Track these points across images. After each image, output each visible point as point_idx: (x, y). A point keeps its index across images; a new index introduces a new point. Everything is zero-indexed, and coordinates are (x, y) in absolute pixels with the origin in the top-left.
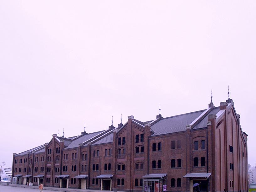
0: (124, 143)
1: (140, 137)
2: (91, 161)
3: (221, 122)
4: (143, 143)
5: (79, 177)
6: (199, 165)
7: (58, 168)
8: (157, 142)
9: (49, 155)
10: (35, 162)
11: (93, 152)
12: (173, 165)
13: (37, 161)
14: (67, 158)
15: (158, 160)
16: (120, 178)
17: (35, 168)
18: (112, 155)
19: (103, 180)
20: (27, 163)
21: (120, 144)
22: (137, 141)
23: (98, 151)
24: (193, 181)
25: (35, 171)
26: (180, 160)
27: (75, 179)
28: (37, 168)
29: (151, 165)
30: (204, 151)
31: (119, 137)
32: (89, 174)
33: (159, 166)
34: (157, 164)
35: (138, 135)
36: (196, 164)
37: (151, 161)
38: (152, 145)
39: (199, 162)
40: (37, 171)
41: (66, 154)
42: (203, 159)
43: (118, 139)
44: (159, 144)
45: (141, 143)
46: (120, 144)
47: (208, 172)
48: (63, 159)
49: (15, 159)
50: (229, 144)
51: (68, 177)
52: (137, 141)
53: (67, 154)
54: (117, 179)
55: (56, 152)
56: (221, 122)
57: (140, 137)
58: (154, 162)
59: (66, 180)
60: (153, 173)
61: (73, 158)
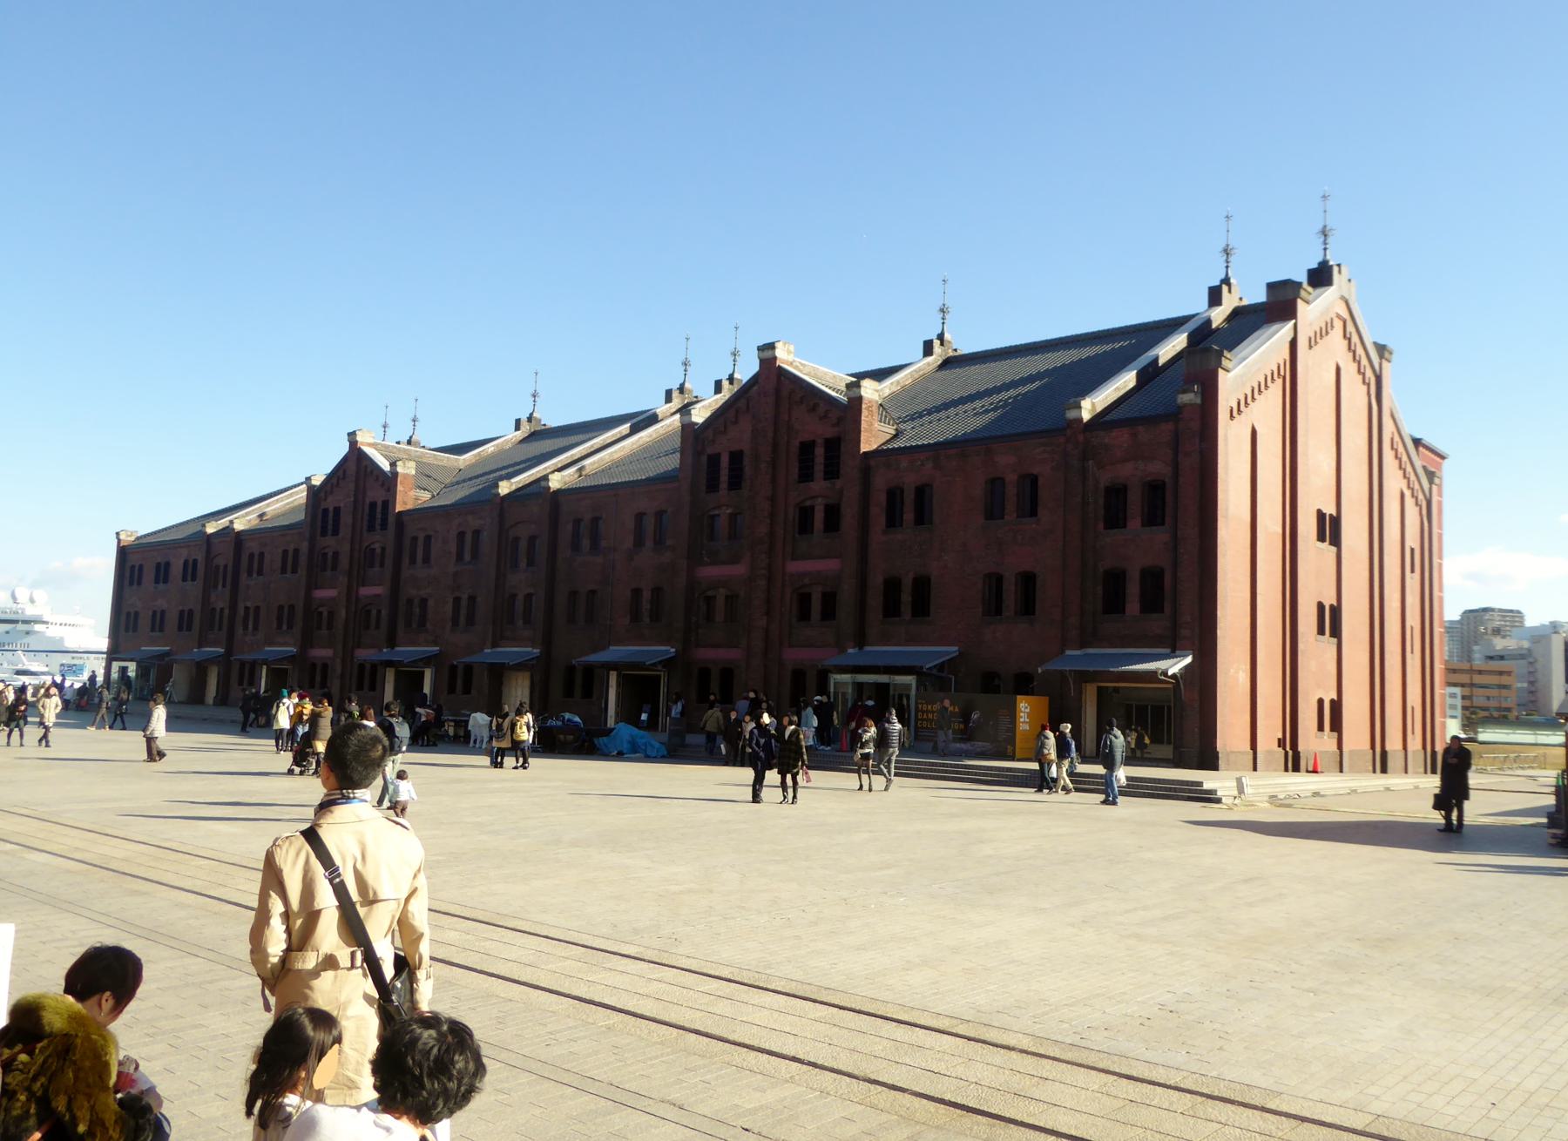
0: (736, 482)
1: (819, 451)
3: (1260, 389)
4: (839, 483)
5: (490, 654)
6: (1133, 606)
7: (374, 612)
8: (910, 481)
9: (329, 542)
10: (244, 576)
11: (570, 527)
12: (994, 606)
13: (260, 573)
14: (426, 560)
15: (911, 576)
17: (247, 608)
18: (669, 542)
19: (618, 676)
20: (199, 582)
21: (713, 486)
22: (806, 475)
23: (595, 520)
24: (1099, 689)
25: (246, 627)
26: (1028, 581)
27: (469, 668)
28: (257, 609)
29: (875, 601)
30: (1161, 535)
31: (710, 451)
32: (547, 642)
33: (921, 607)
34: (906, 597)
35: (813, 443)
36: (1114, 602)
37: (877, 580)
38: (883, 498)
39: (1133, 590)
40: (256, 628)
41: (421, 536)
42: (1153, 580)
43: (704, 458)
44: (922, 492)
45: (827, 484)
46: (713, 486)
47: (1178, 645)
48: (406, 560)
49: (129, 565)
50: (1315, 497)
51: (428, 660)
52: (806, 475)
53: (428, 538)
55: (365, 523)
56: (1260, 389)
57: (819, 451)
58: (892, 587)
59: (422, 674)
60: (885, 639)
61: (460, 556)
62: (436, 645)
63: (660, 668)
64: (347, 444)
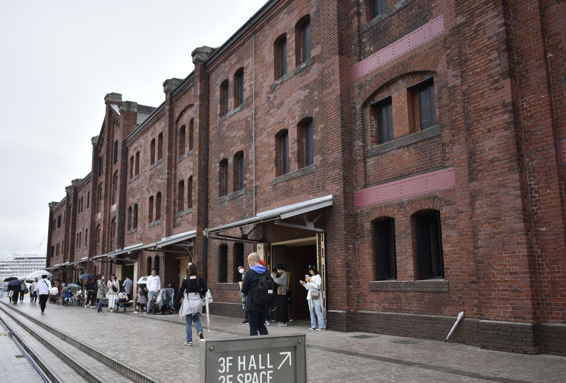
2: (213, 147)
16: (401, 205)
53: (138, 154)
54: (368, 226)
59: (133, 267)
62: (141, 242)
63: (310, 227)
64: (105, 106)
